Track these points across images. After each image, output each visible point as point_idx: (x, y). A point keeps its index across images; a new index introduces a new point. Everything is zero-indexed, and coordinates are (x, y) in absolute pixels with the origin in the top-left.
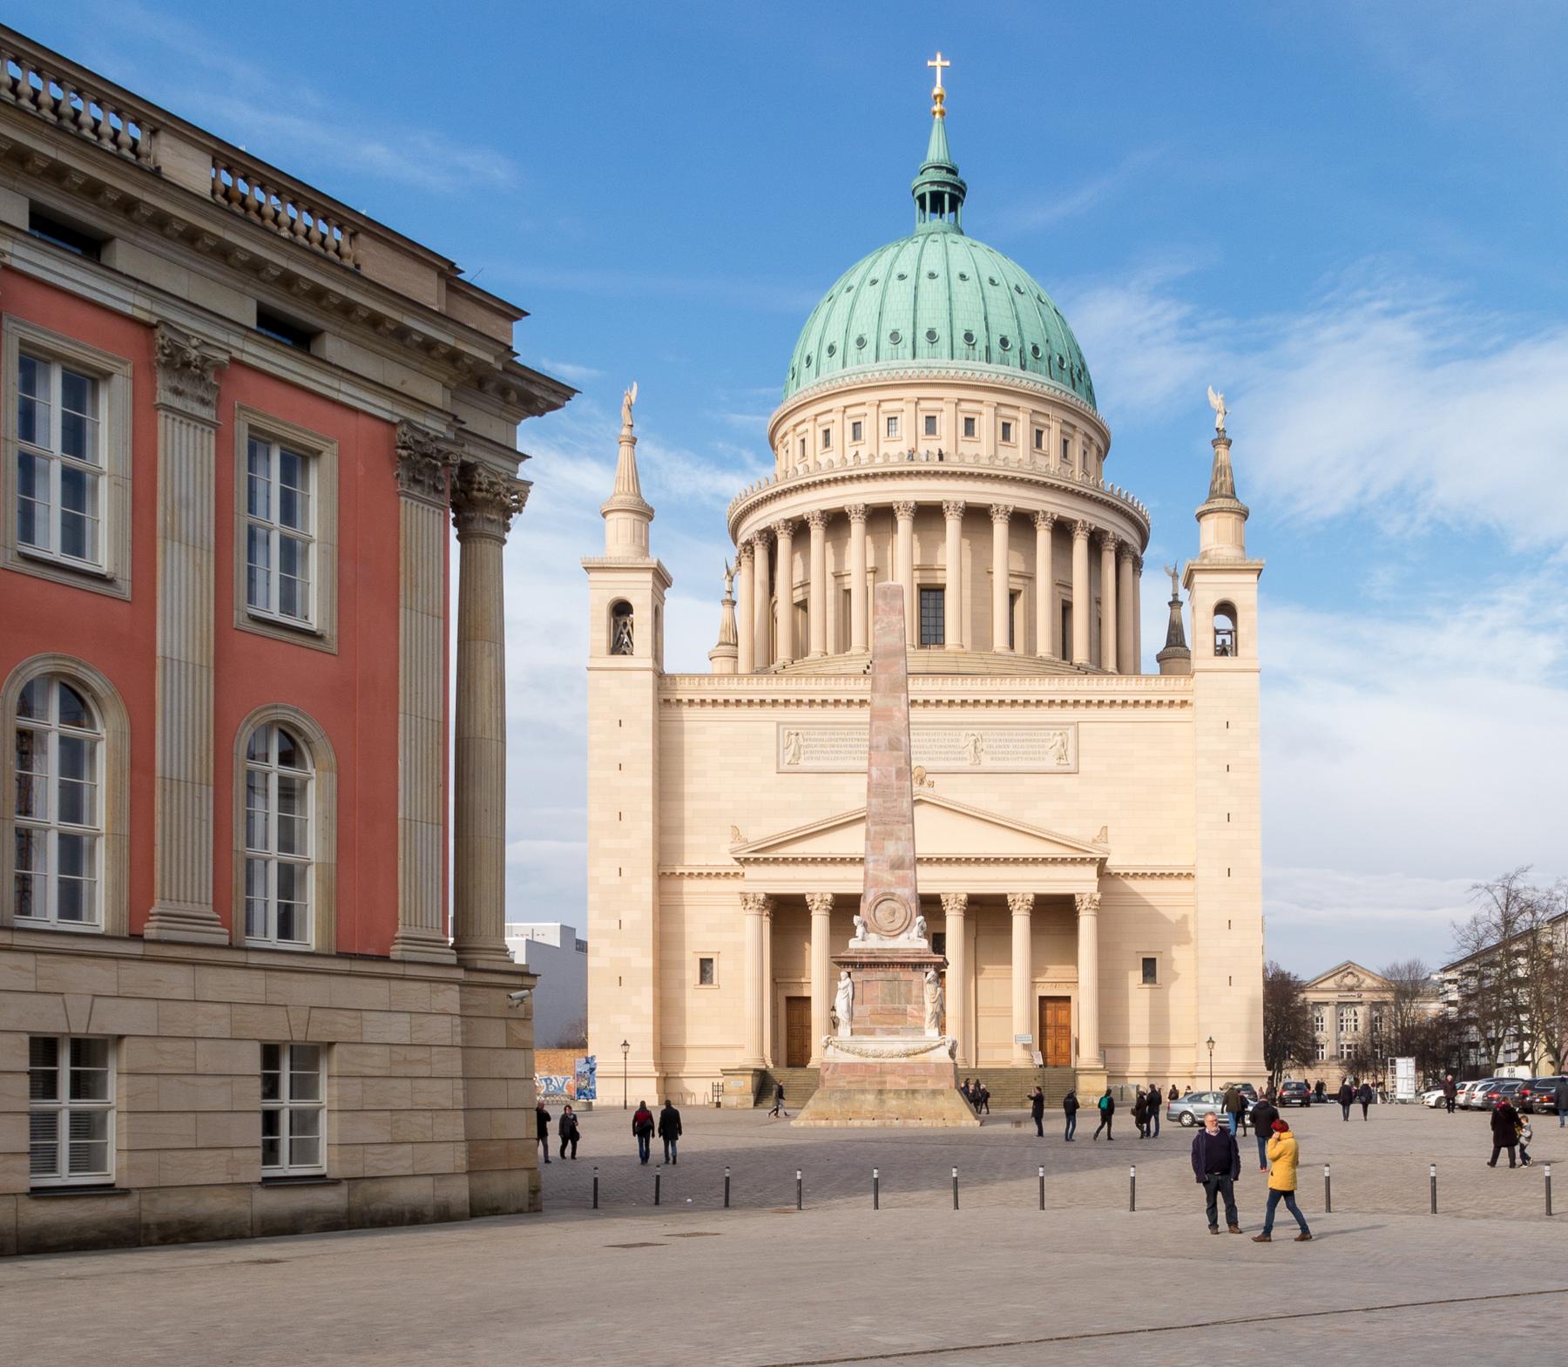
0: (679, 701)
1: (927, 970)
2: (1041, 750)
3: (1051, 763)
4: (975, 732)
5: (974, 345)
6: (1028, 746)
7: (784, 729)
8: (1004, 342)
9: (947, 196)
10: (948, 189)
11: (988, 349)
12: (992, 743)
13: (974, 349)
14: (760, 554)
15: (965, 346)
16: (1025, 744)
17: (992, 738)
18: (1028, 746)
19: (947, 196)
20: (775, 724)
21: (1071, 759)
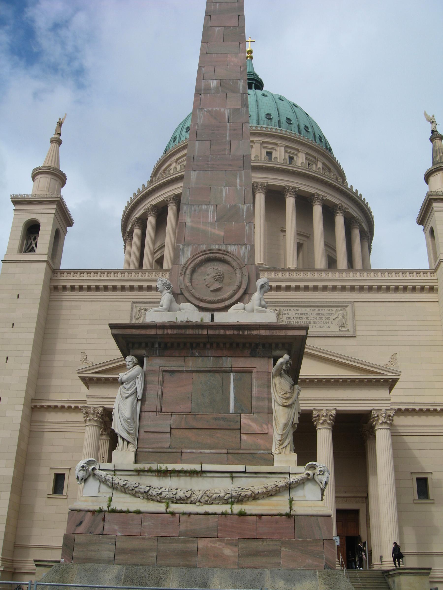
0: (64, 288)
1: (277, 353)
2: (327, 321)
3: (335, 330)
4: (278, 309)
5: (271, 119)
6: (317, 318)
7: (138, 306)
8: (289, 120)
9: (253, 85)
10: (254, 82)
11: (279, 122)
12: (289, 316)
13: (271, 121)
14: (137, 233)
15: (266, 119)
16: (315, 316)
17: (290, 312)
18: (317, 318)
19: (253, 85)
20: (130, 303)
21: (349, 326)
